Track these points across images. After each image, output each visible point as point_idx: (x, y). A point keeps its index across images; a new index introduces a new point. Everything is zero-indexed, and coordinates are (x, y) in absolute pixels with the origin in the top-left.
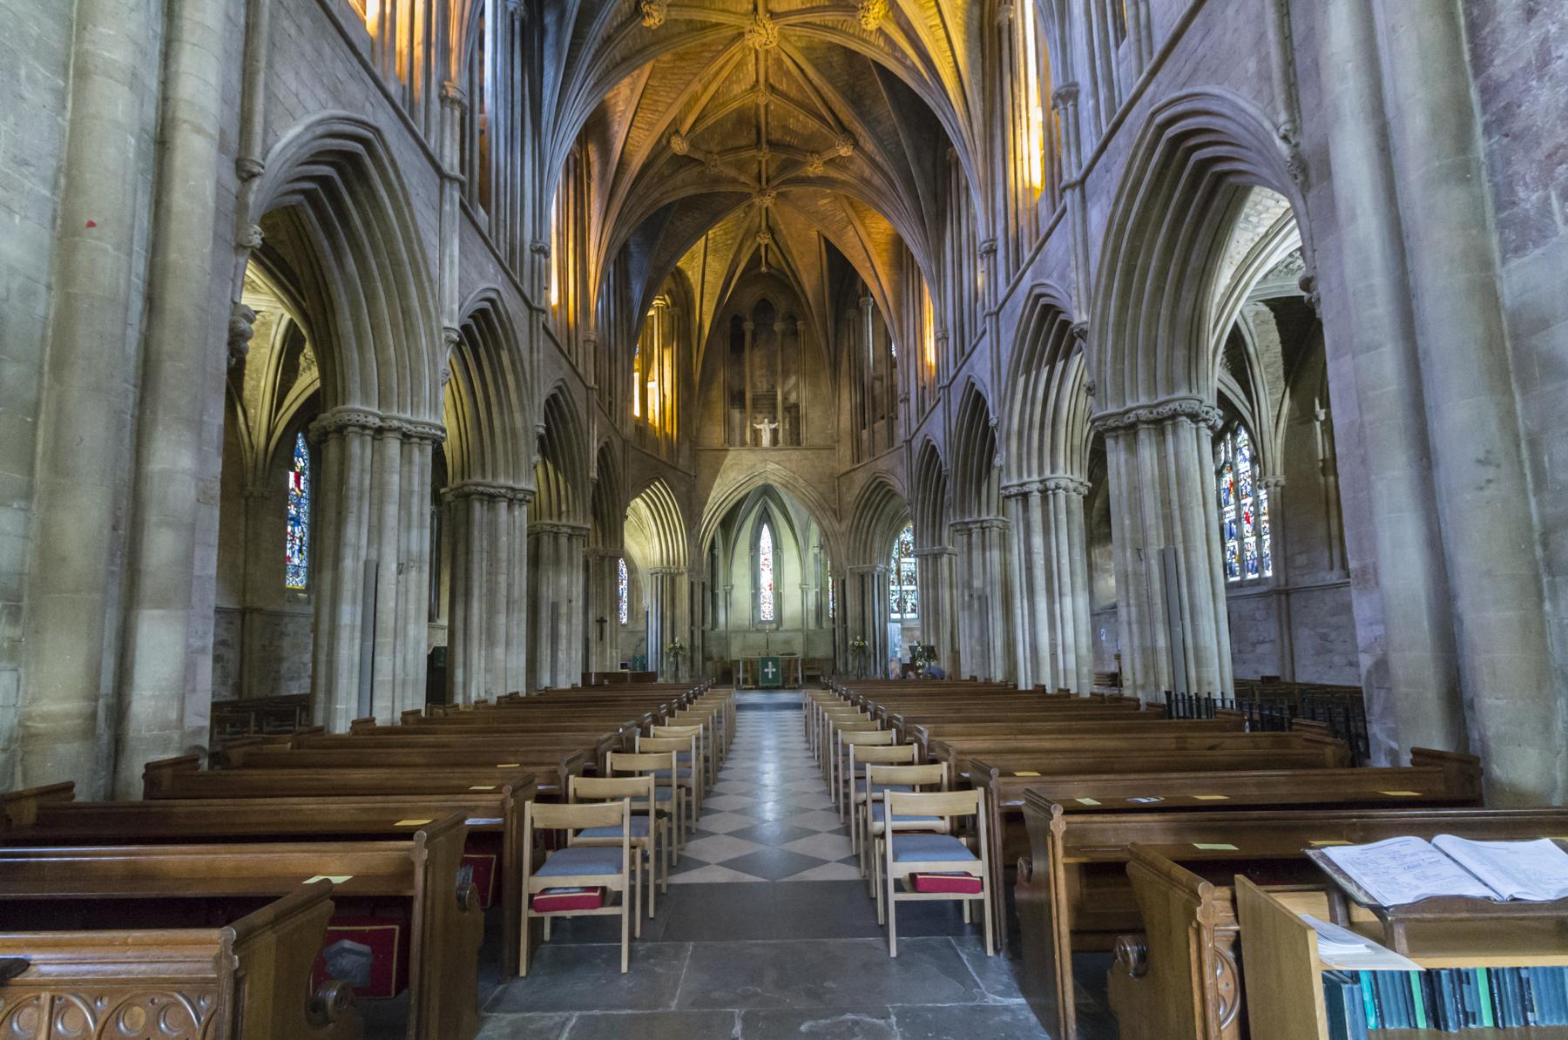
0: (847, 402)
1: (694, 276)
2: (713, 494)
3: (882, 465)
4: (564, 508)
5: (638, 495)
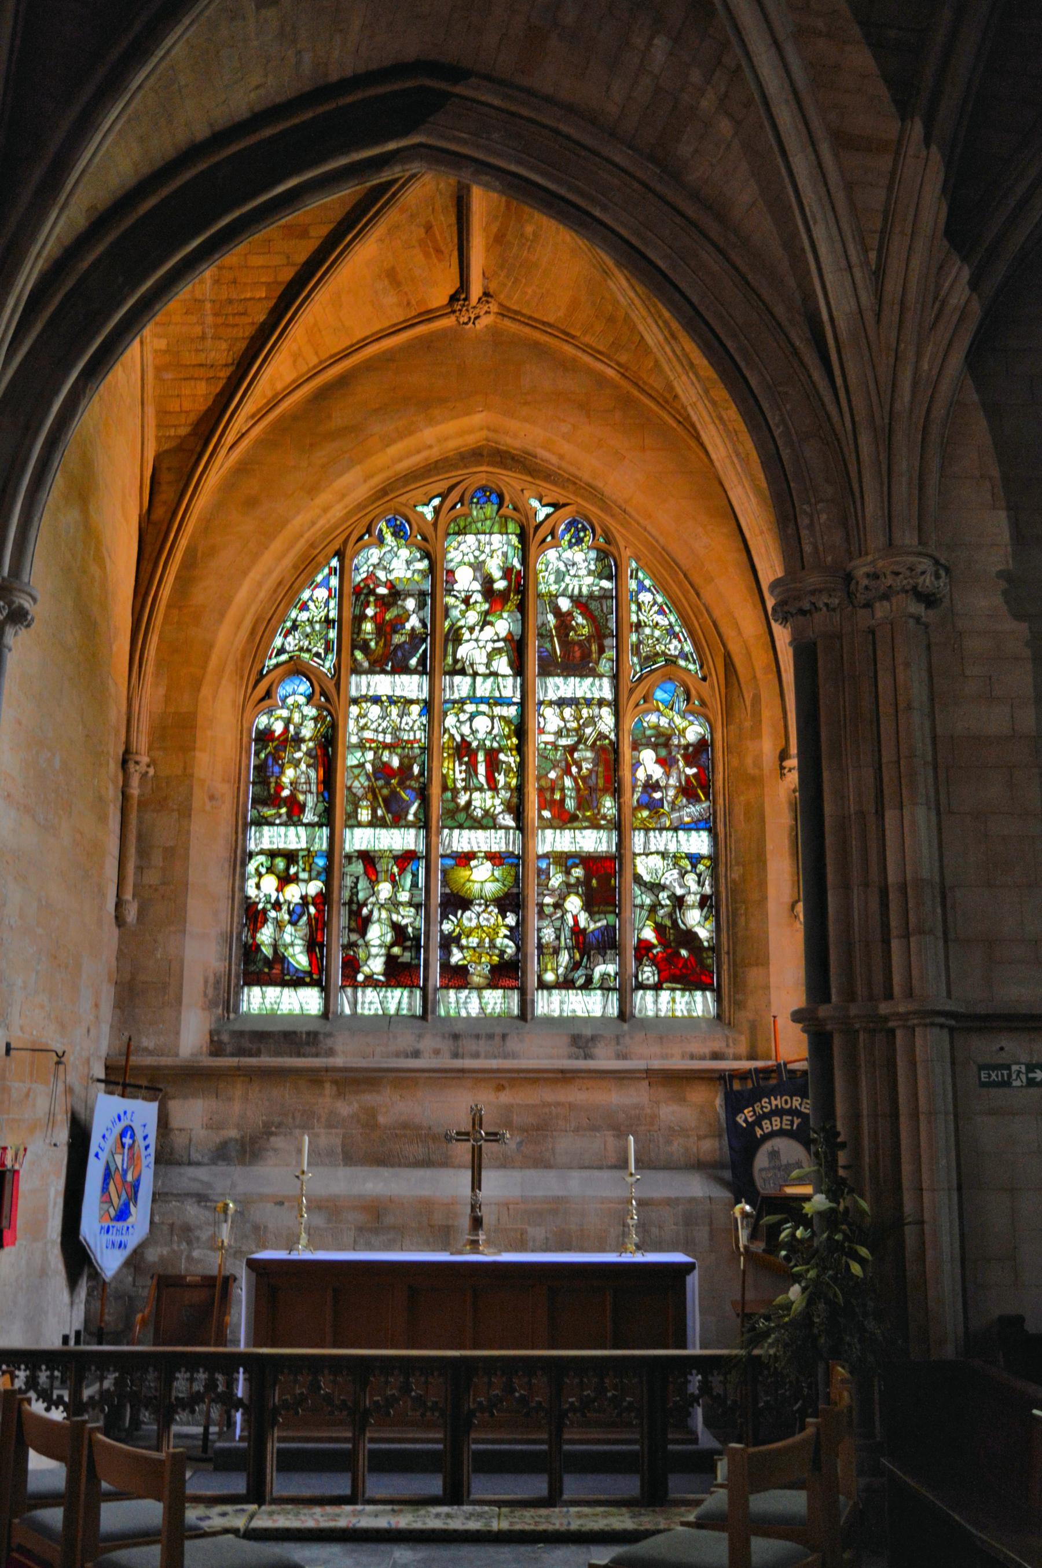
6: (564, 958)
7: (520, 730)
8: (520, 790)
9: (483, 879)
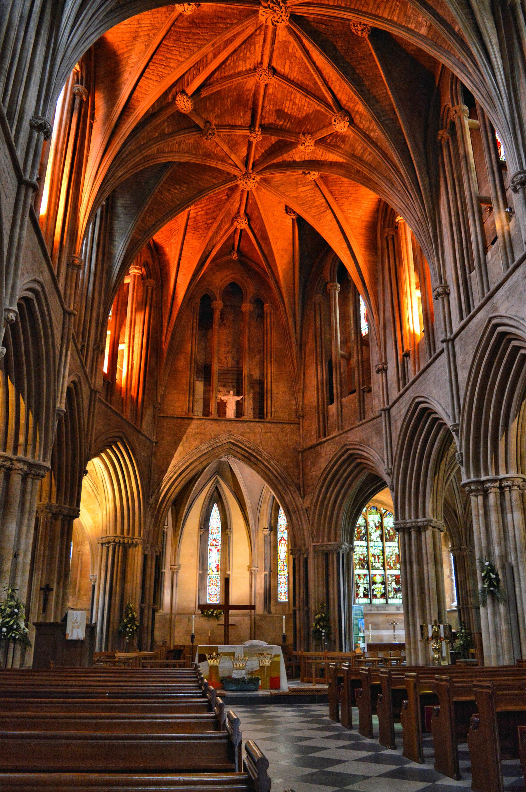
0: (314, 377)
1: (171, 253)
2: (174, 462)
3: (355, 437)
4: (22, 439)
5: (97, 455)
6: (392, 593)
7: (383, 552)
8: (384, 563)
9: (378, 579)
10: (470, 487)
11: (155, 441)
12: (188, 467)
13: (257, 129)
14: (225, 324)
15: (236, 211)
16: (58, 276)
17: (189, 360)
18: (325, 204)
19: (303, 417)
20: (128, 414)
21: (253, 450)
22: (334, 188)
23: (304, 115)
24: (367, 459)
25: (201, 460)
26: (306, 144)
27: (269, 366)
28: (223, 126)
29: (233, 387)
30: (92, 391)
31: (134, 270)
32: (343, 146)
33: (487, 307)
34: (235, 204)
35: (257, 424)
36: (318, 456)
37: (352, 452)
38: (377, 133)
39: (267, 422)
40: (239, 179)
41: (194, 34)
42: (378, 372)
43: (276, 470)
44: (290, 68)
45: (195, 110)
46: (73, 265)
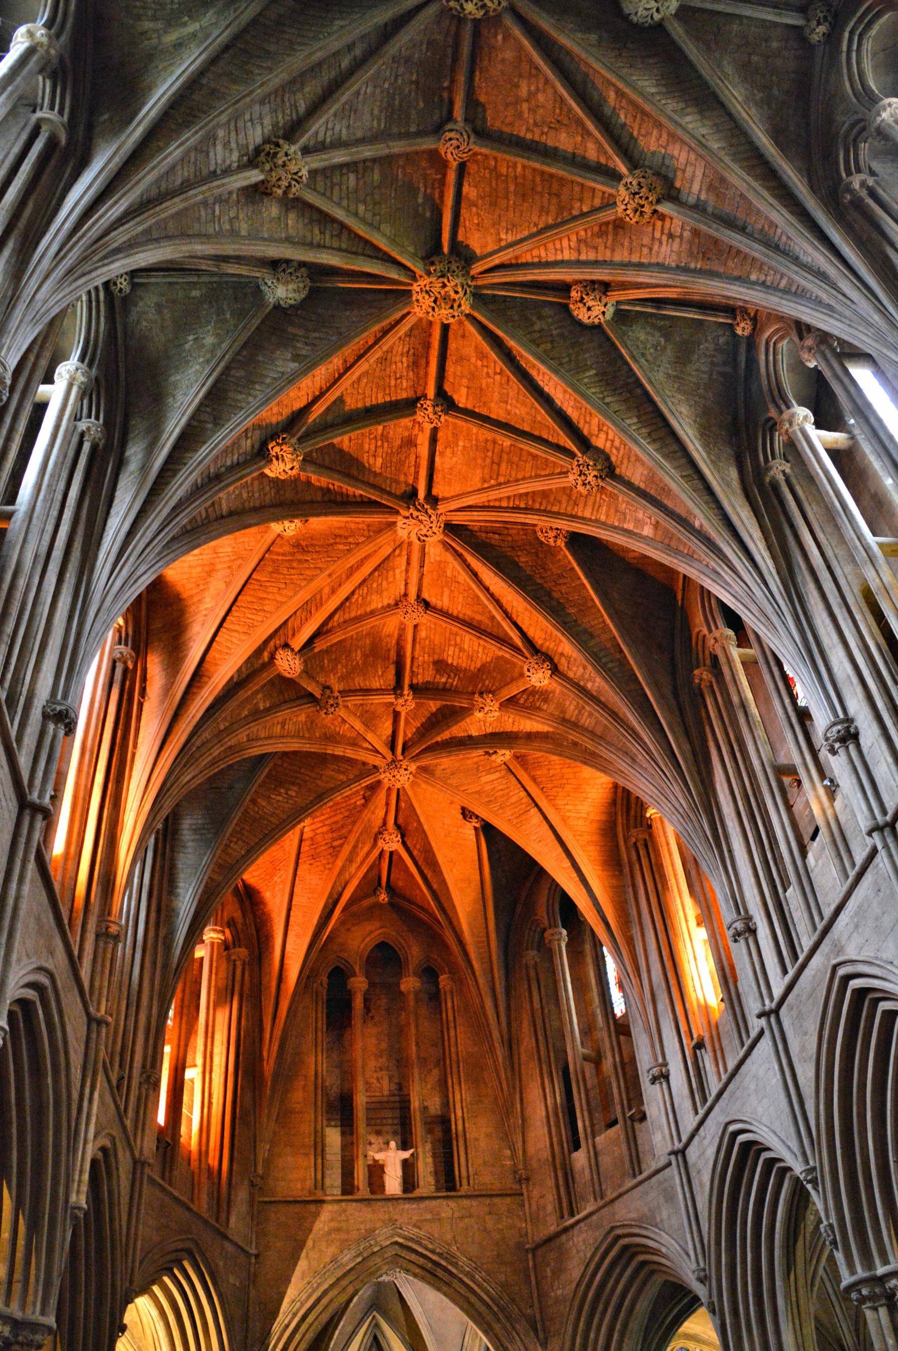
0: (539, 1102)
1: (275, 901)
2: (291, 1292)
3: (627, 1210)
5: (145, 1290)
10: (859, 1291)
11: (253, 1251)
12: (318, 1300)
13: (406, 692)
14: (372, 1018)
15: (379, 822)
16: (80, 957)
17: (311, 1088)
18: (526, 800)
19: (527, 1179)
20: (203, 1204)
21: (440, 1255)
22: (539, 773)
23: (479, 665)
24: (656, 1252)
25: (344, 1283)
26: (487, 709)
27: (457, 1088)
28: (350, 691)
29: (395, 1133)
30: (135, 1162)
31: (211, 935)
32: (545, 707)
33: (825, 947)
34: (377, 812)
35: (444, 1202)
36: (563, 1255)
37: (626, 1241)
38: (597, 683)
39: (461, 1197)
40: (381, 770)
41: (300, 561)
42: (654, 1080)
43: (487, 1293)
44: (451, 598)
45: (307, 672)
46: (107, 935)
